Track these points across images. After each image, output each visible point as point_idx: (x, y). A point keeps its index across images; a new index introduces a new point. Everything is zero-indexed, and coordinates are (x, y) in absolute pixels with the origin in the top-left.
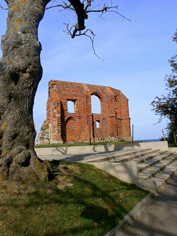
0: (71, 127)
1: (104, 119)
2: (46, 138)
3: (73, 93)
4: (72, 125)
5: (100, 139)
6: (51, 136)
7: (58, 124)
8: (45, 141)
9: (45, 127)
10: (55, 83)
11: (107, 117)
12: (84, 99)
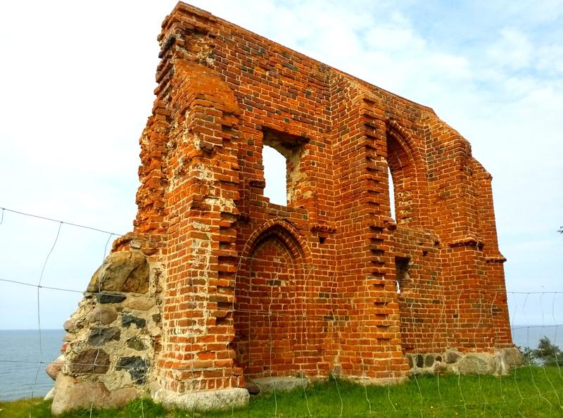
0: (271, 283)
1: (425, 253)
2: (126, 363)
3: (294, 104)
4: (281, 277)
5: (415, 363)
6: (157, 346)
7: (222, 259)
8: (111, 386)
9: (119, 278)
10: (200, 24)
11: (437, 243)
12: (347, 137)
